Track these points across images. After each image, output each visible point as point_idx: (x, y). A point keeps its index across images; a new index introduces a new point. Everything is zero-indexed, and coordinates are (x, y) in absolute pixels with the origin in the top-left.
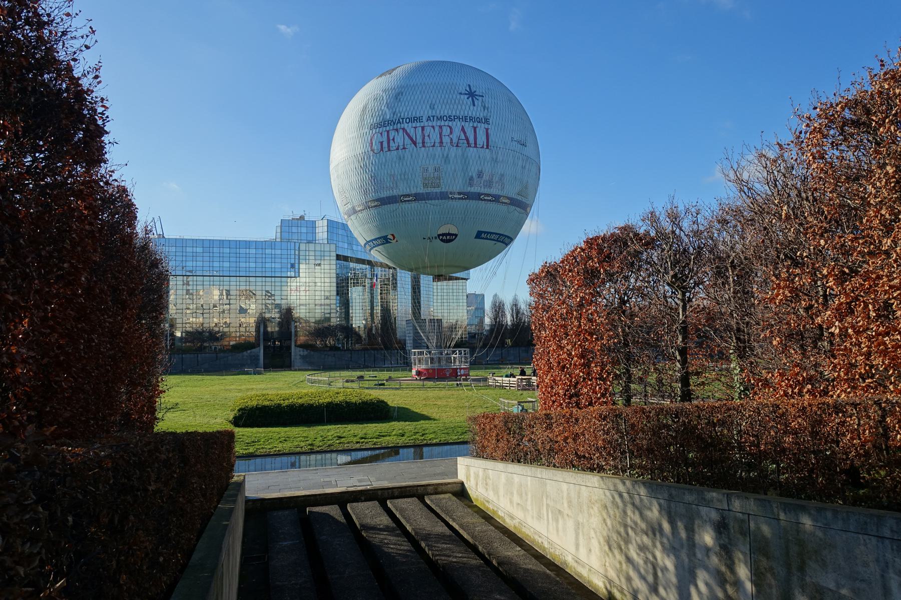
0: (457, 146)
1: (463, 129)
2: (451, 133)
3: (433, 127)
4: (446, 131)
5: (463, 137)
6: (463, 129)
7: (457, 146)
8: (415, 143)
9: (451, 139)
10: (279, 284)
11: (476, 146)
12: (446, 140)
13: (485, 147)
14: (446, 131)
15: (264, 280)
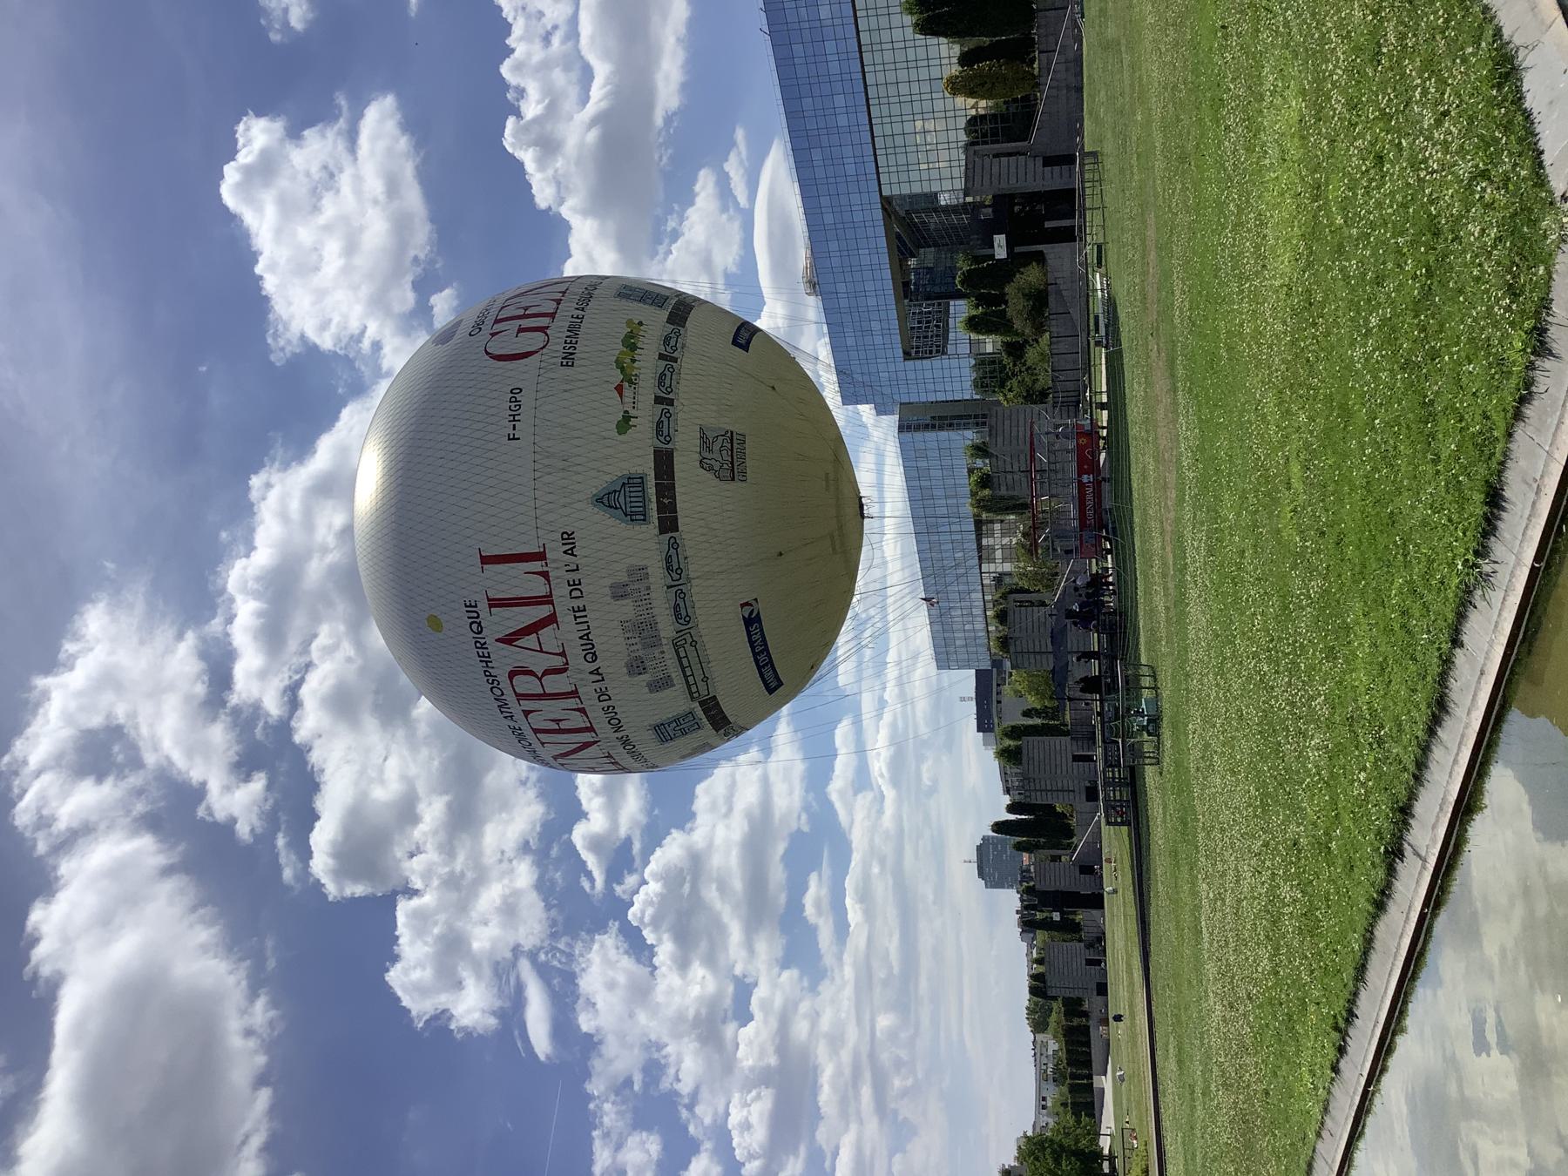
0: (563, 654)
1: (509, 640)
2: (531, 673)
3: (527, 713)
4: (525, 684)
5: (530, 641)
6: (509, 640)
7: (563, 654)
8: (586, 745)
9: (546, 672)
10: (882, 89)
11: (547, 600)
12: (554, 684)
13: (537, 566)
14: (525, 684)
15: (871, 68)
